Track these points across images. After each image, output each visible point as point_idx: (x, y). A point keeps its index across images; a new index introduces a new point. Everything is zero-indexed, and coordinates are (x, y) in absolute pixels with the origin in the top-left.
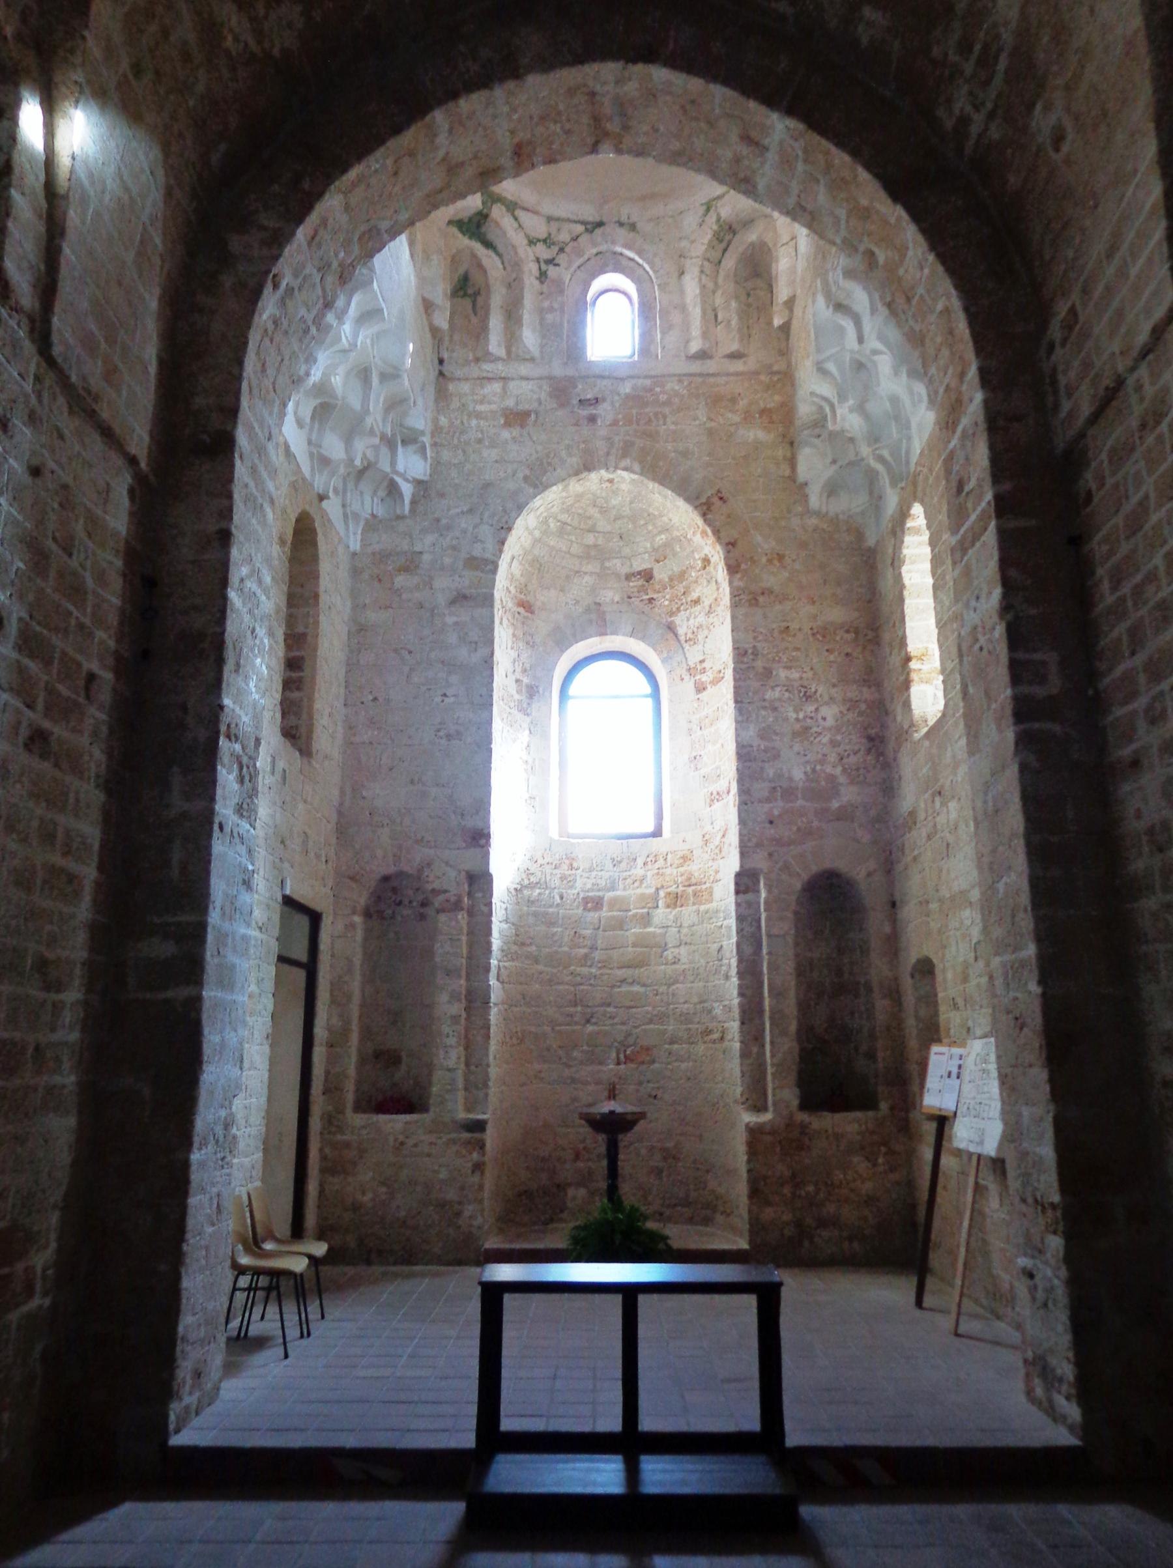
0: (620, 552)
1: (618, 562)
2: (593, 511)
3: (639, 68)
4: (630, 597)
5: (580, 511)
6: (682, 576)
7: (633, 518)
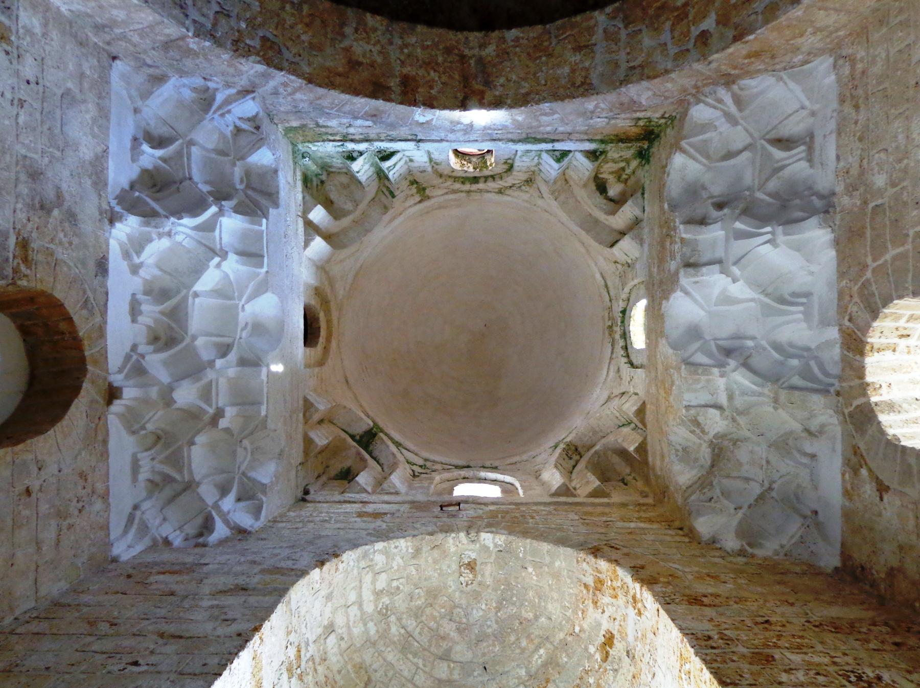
2: (448, 628)
3: (496, 34)
7: (500, 636)
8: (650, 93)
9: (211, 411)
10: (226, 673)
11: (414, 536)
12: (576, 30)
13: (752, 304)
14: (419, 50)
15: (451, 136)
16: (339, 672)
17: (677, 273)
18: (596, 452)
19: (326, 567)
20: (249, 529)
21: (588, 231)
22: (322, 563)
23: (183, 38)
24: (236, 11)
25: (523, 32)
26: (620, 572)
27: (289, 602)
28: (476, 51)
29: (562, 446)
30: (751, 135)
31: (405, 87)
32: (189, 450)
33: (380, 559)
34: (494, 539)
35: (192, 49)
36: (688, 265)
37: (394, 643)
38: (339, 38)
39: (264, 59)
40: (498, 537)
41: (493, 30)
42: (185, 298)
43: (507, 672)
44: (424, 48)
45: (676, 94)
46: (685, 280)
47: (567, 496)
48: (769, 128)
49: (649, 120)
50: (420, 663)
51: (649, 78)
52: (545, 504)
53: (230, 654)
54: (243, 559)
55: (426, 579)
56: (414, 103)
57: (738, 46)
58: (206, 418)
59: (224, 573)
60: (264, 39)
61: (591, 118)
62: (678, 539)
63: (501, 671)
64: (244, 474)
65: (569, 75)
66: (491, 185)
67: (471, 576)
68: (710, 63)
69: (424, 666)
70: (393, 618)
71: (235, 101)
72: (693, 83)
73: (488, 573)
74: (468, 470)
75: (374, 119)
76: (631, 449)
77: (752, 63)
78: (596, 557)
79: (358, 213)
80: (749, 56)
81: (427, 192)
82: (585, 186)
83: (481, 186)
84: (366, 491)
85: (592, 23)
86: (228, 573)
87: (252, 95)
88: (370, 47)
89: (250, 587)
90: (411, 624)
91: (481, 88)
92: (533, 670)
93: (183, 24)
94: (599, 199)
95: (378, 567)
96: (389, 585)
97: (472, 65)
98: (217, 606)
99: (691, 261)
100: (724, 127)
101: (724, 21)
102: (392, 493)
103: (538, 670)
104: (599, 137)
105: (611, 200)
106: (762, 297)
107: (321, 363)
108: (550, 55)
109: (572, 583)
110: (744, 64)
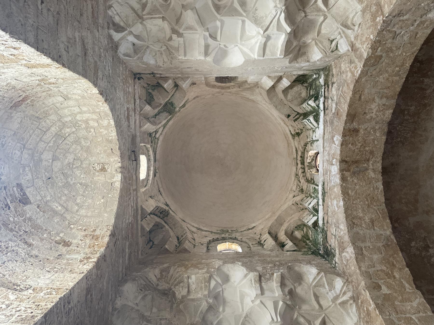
0: (38, 178)
1: (29, 177)
2: (70, 158)
4: (5, 188)
5: (71, 150)
6: (37, 227)
7: (67, 185)
8: (349, 258)
9: (181, 31)
10: (39, 53)
11: (118, 140)
12: (382, 219)
13: (241, 310)
14: (372, 137)
15: (326, 153)
16: (44, 103)
17: (256, 270)
18: (165, 226)
19: (99, 95)
20: (118, 51)
21: (276, 220)
22: (101, 94)
23: (382, 14)
24: (396, 42)
25: (381, 191)
26: (102, 249)
27: (80, 79)
28: (371, 167)
29: (167, 208)
30: (326, 309)
31: (353, 131)
32: (159, 18)
33: (105, 123)
34: (118, 181)
35: (376, 19)
36: (260, 277)
37: (61, 131)
38: (380, 96)
39: (370, 57)
40: (120, 183)
41: (382, 176)
42: (241, 15)
43: (48, 190)
44: (374, 140)
45: (349, 271)
46: (252, 275)
47: (141, 215)
48: (331, 318)
49: (334, 256)
50: (51, 144)
51: (357, 258)
52: (137, 204)
53: (50, 53)
54: (102, 50)
55: (95, 146)
56: (344, 135)
57: (373, 306)
58: (176, 28)
59: (94, 42)
60: (381, 57)
61: (335, 227)
62: (121, 275)
63: (48, 187)
64: (148, 47)
65: (358, 216)
66: (300, 171)
67: (98, 169)
68: (364, 290)
69: (49, 147)
70: (74, 130)
71: (348, 41)
72: (354, 280)
73: (100, 178)
74: (154, 161)
75: (336, 114)
76: (166, 246)
77: (364, 312)
78: (110, 236)
79: (286, 102)
80: (368, 310)
81: (297, 138)
82: (300, 220)
83: (300, 166)
84: (141, 111)
85: (386, 228)
86: (94, 43)
87: (350, 49)
88: (375, 112)
89: (87, 57)
90: (71, 139)
91: (352, 170)
92: (49, 204)
93: (390, 15)
94: (293, 226)
95: (101, 122)
96: (92, 127)
97: (364, 165)
98: (76, 41)
99: (262, 278)
100: (331, 295)
101: (387, 298)
102: (140, 124)
103: (50, 206)
104: (325, 229)
105: (293, 232)
106: (244, 315)
107: (207, 84)
108: (369, 206)
109: (96, 223)
110: (364, 307)
